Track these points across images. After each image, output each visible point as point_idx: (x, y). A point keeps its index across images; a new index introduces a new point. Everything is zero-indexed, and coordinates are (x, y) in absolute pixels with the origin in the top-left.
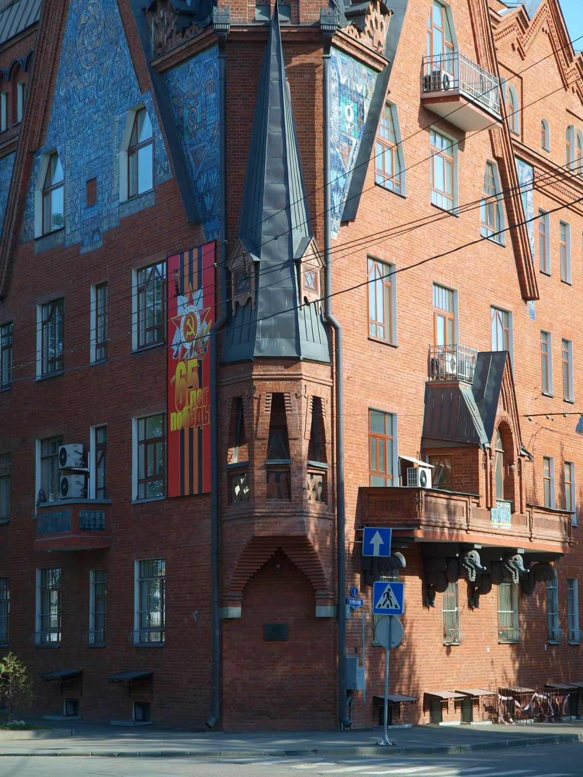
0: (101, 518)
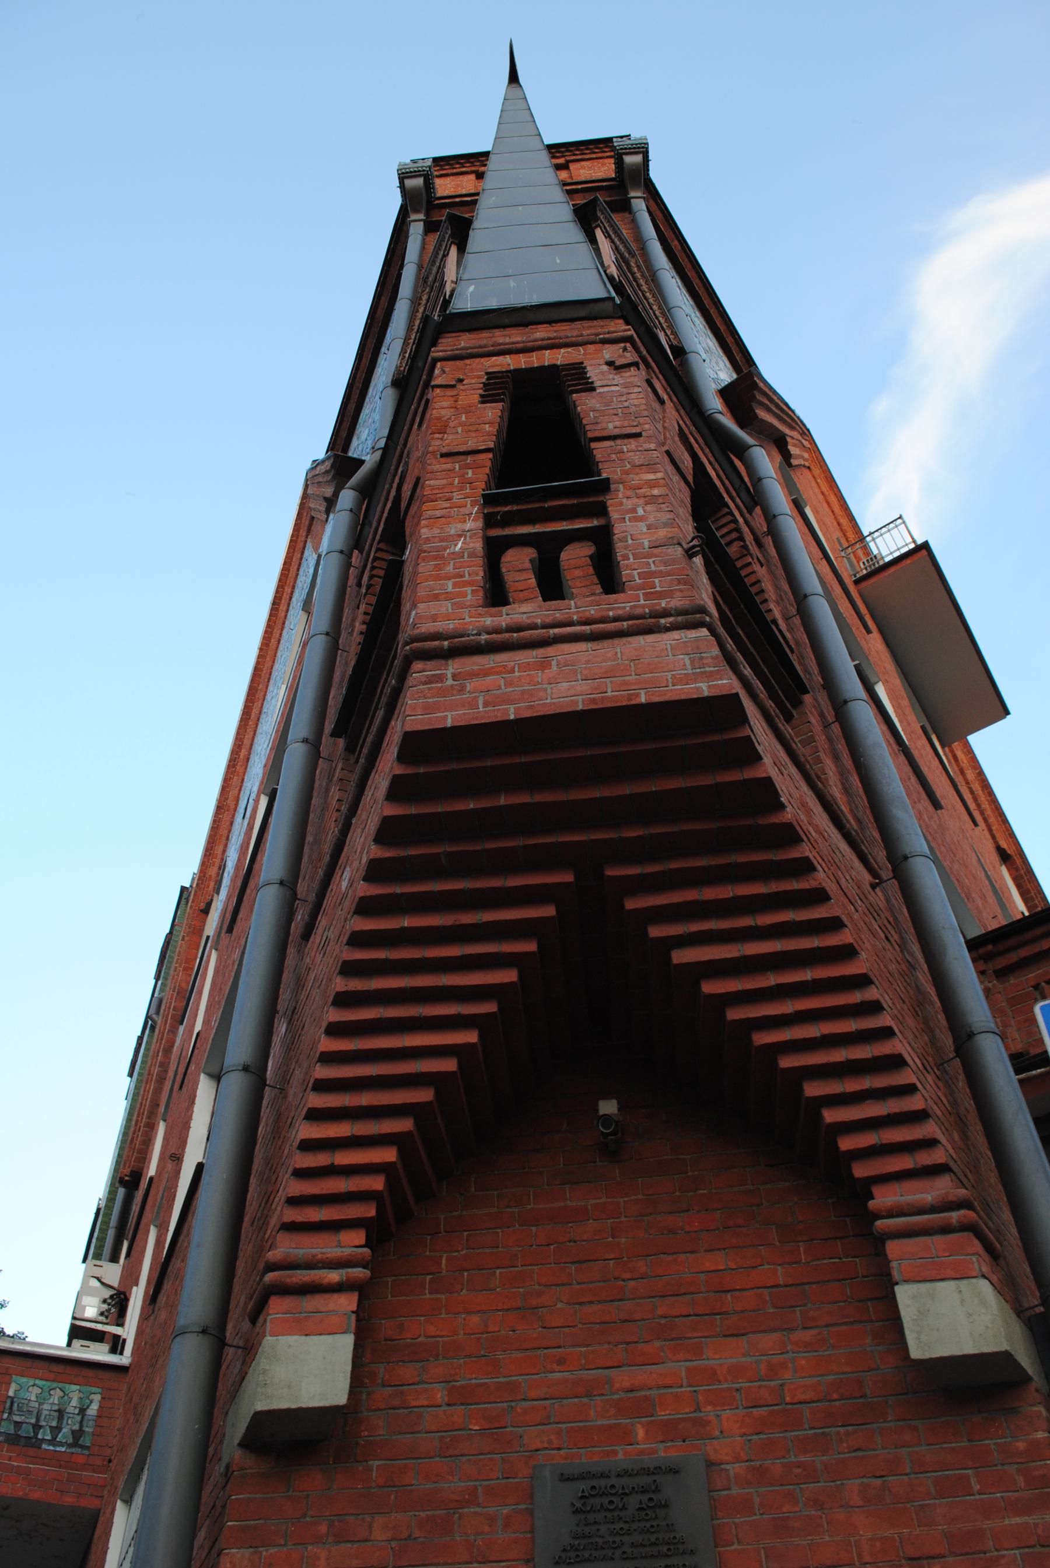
0: (82, 1411)
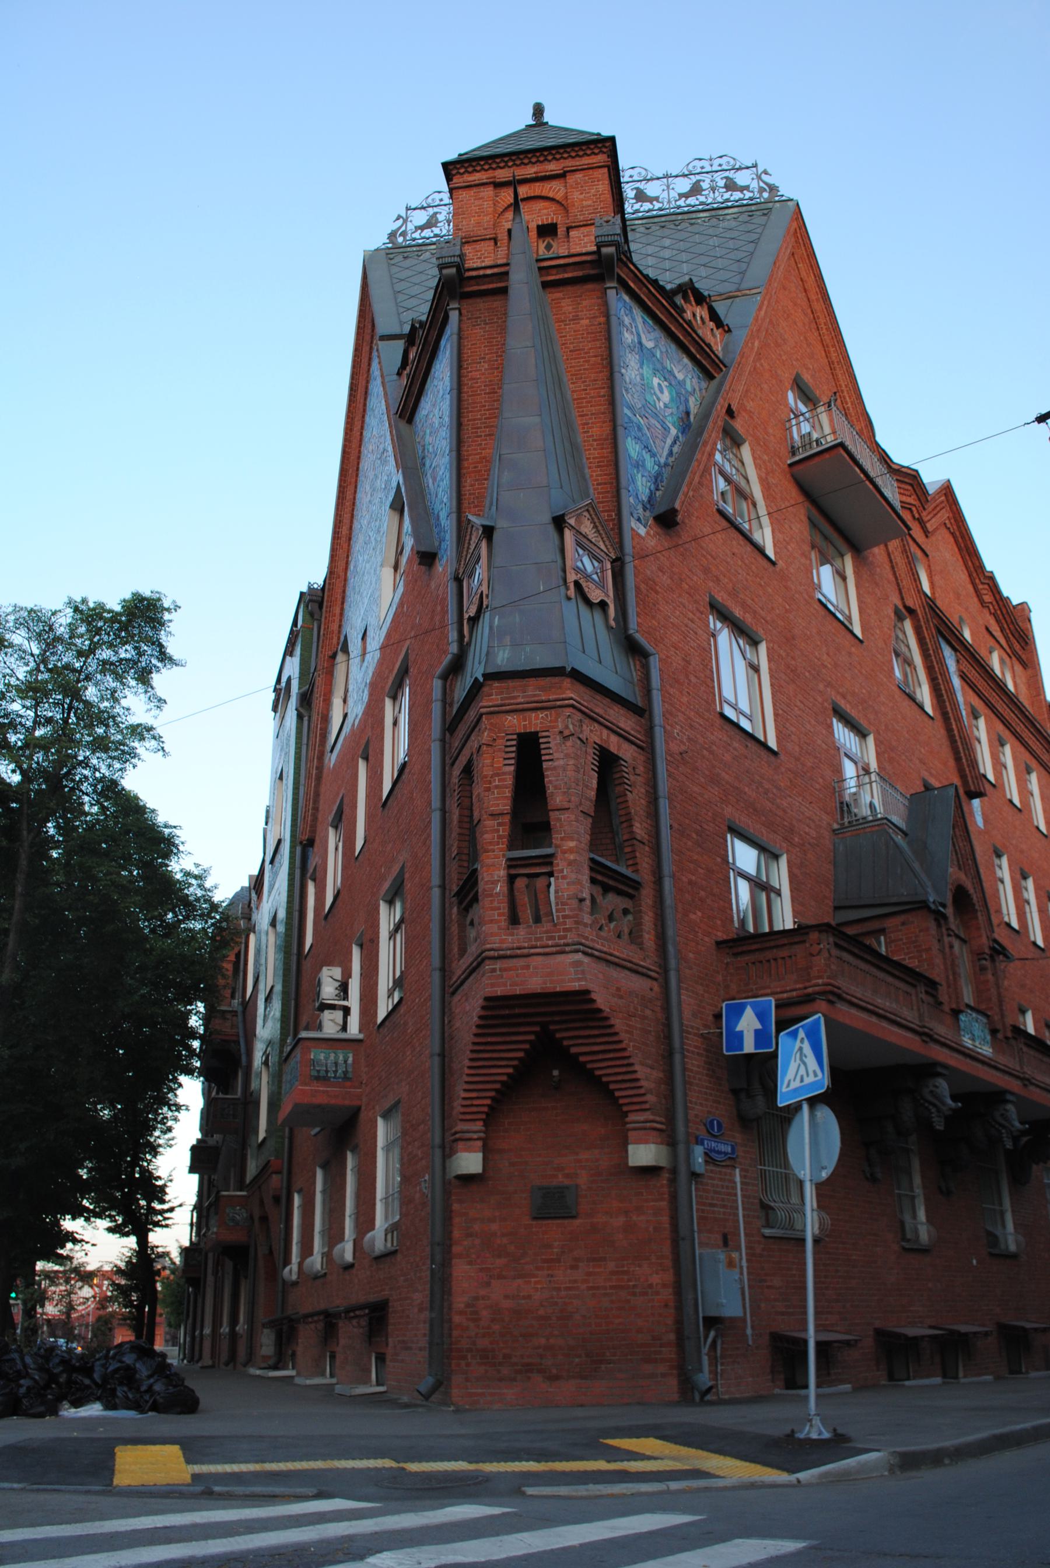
0: (346, 1062)
